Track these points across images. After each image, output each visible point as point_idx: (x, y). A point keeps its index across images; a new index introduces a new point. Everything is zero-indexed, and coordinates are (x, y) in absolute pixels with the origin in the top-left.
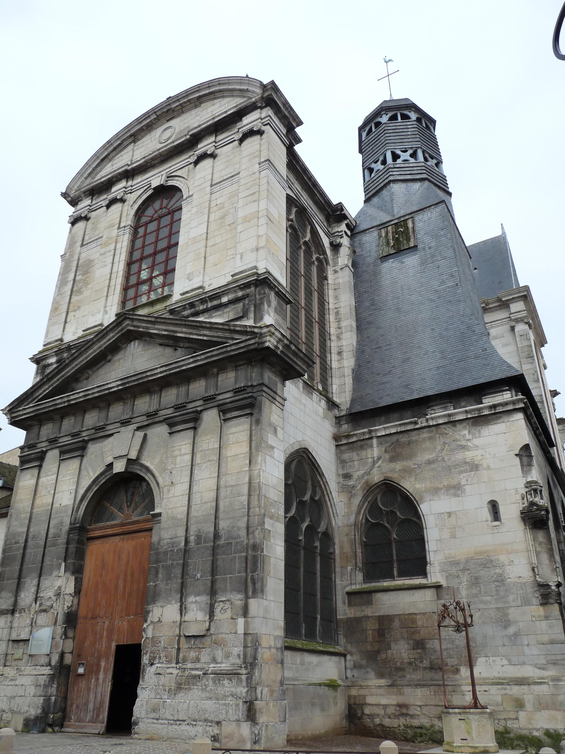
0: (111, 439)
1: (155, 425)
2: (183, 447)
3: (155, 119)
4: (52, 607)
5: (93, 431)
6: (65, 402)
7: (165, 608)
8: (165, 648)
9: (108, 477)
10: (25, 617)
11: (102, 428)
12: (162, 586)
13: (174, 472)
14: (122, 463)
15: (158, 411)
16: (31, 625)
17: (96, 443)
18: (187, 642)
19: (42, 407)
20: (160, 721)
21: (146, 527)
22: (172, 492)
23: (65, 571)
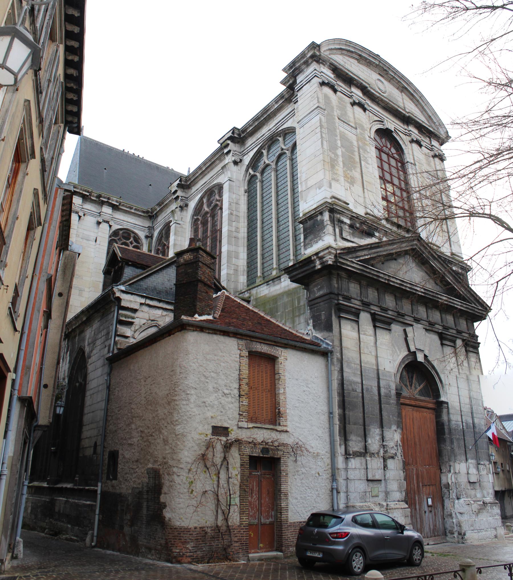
3: (377, 65)
6: (386, 279)
10: (376, 460)
12: (456, 450)
16: (384, 467)
18: (470, 486)
19: (368, 270)
22: (450, 390)
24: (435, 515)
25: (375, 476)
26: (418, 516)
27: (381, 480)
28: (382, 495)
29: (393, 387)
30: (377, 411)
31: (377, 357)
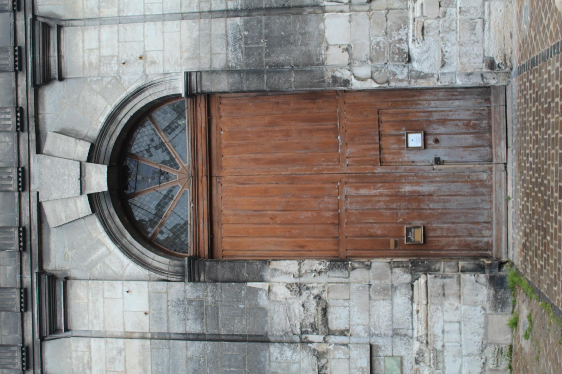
0: (47, 208)
1: (40, 117)
2: (87, 47)
4: (318, 297)
5: (26, 257)
7: (331, 42)
8: (386, 33)
9: (112, 210)
11: (24, 233)
13: (124, 58)
14: (93, 174)
15: (17, 107)
17: (49, 249)
20: (486, 17)
21: (204, 125)
23: (261, 280)
24: (443, 122)
25: (363, 368)
26: (445, 188)
27: (371, 346)
28: (400, 349)
29: (180, 289)
30: (236, 346)
31: (128, 336)
